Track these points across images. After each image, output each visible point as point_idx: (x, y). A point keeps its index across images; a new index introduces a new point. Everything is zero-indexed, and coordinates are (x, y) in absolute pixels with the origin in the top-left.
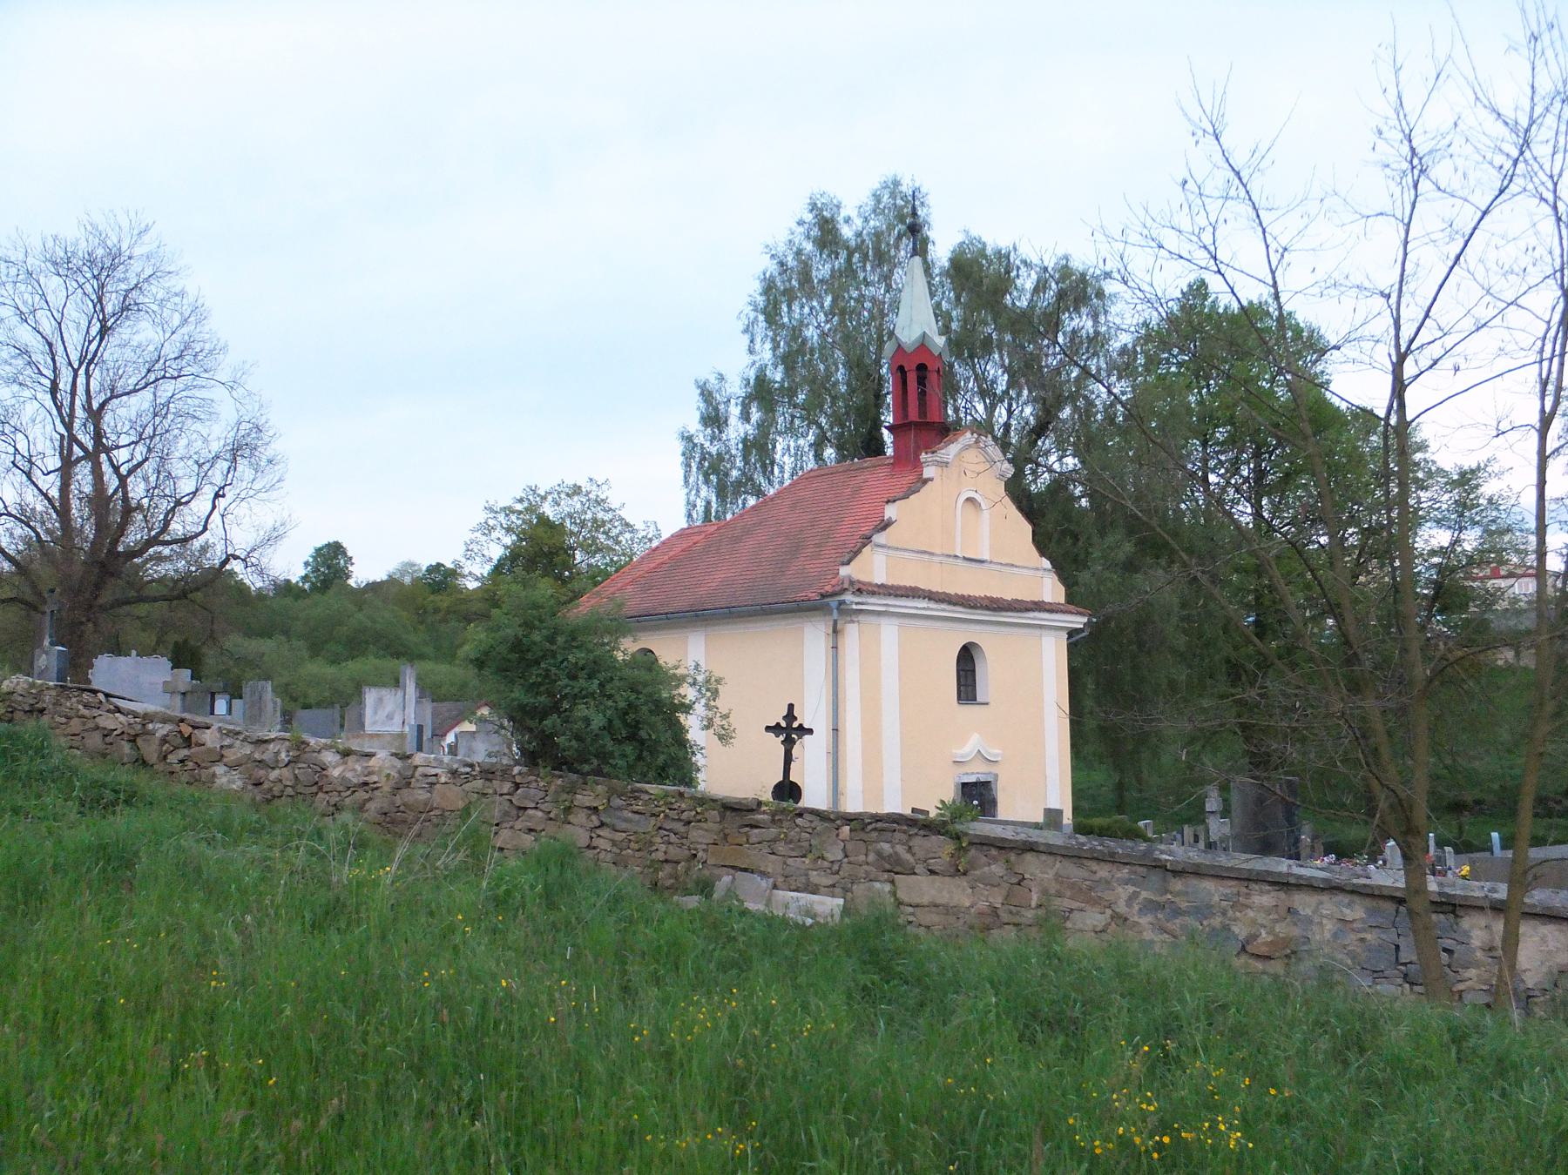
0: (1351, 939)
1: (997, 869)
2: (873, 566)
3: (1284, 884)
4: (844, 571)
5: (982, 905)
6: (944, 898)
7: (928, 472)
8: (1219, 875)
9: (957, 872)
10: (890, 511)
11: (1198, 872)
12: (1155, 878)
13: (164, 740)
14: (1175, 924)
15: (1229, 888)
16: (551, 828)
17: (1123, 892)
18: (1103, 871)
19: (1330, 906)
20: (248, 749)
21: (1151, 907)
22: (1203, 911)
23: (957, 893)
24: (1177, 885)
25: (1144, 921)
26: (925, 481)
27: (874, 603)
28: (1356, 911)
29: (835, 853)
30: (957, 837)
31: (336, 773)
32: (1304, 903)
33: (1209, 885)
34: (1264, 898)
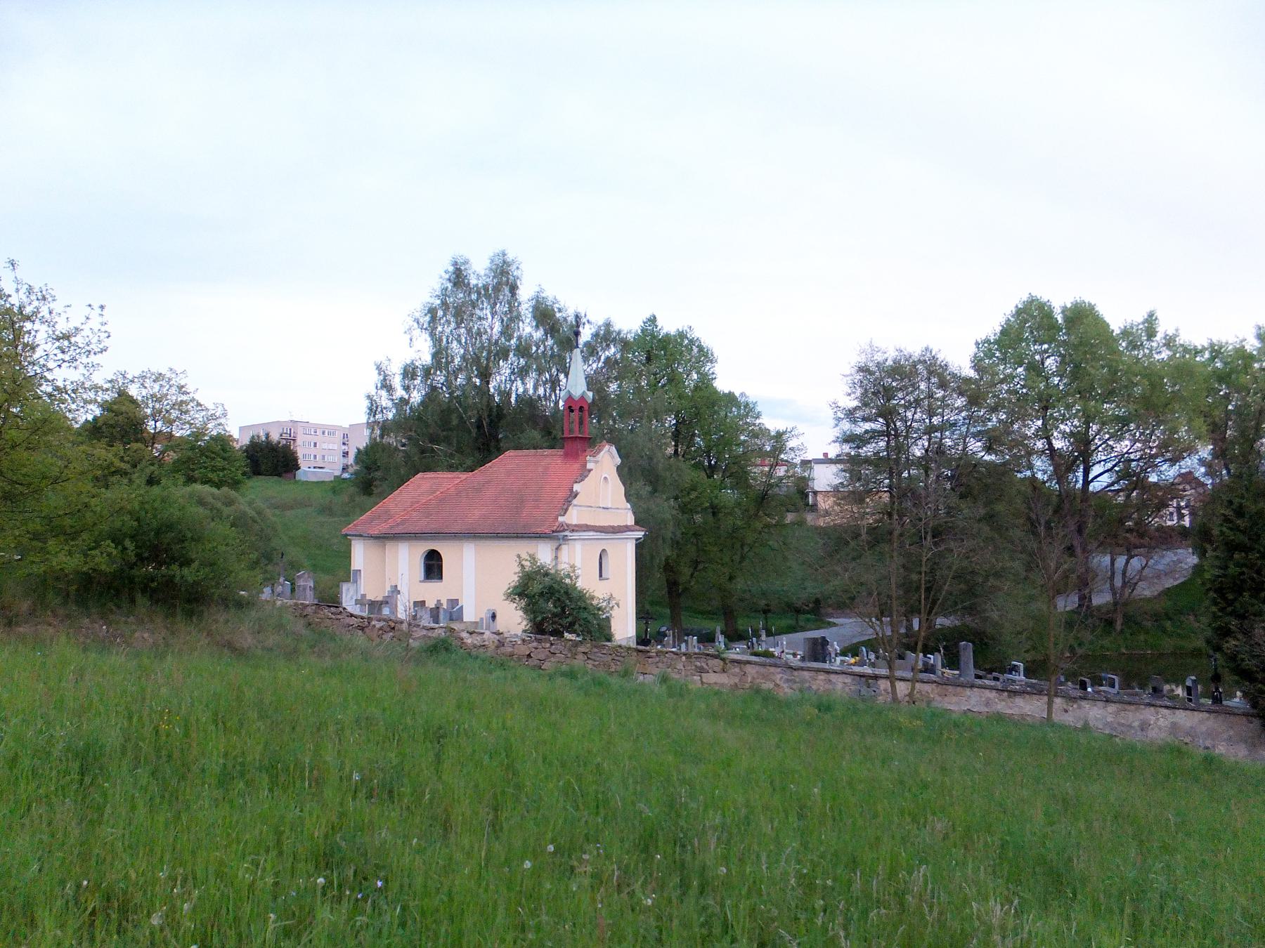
0: (847, 689)
1: (737, 670)
2: (573, 516)
3: (828, 672)
4: (561, 519)
5: (732, 682)
6: (719, 681)
7: (589, 466)
8: (809, 669)
9: (724, 671)
10: (576, 487)
11: (802, 669)
12: (788, 671)
13: (381, 629)
14: (795, 686)
15: (812, 674)
16: (568, 661)
17: (779, 676)
18: (772, 669)
19: (841, 678)
20: (425, 632)
21: (788, 681)
22: (803, 681)
23: (723, 679)
24: (796, 673)
25: (785, 686)
26: (590, 471)
27: (576, 535)
28: (848, 680)
29: (680, 666)
30: (723, 660)
31: (469, 641)
32: (832, 677)
33: (806, 673)
34: (822, 677)
